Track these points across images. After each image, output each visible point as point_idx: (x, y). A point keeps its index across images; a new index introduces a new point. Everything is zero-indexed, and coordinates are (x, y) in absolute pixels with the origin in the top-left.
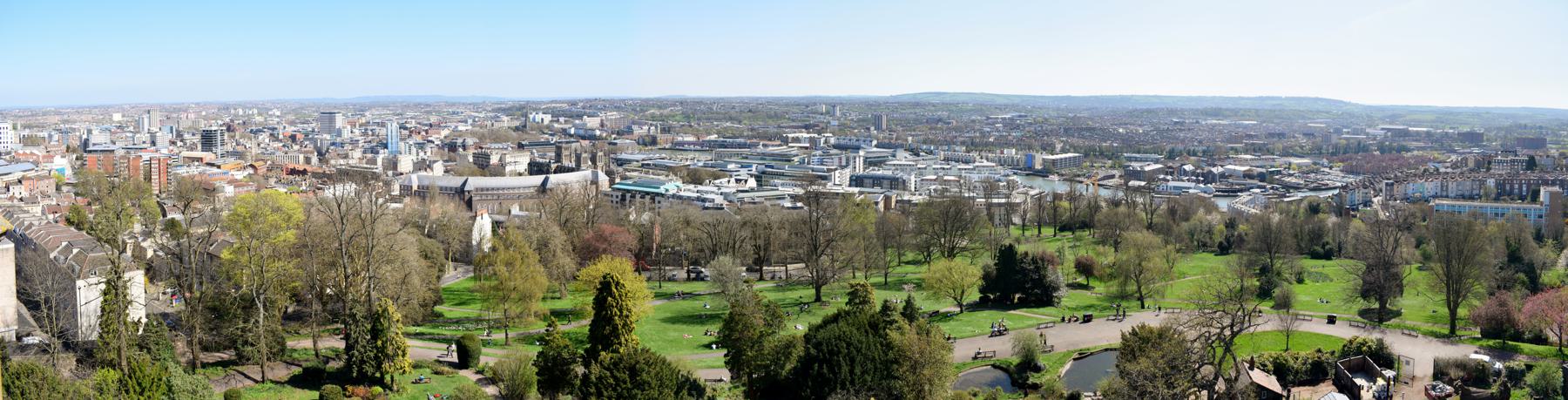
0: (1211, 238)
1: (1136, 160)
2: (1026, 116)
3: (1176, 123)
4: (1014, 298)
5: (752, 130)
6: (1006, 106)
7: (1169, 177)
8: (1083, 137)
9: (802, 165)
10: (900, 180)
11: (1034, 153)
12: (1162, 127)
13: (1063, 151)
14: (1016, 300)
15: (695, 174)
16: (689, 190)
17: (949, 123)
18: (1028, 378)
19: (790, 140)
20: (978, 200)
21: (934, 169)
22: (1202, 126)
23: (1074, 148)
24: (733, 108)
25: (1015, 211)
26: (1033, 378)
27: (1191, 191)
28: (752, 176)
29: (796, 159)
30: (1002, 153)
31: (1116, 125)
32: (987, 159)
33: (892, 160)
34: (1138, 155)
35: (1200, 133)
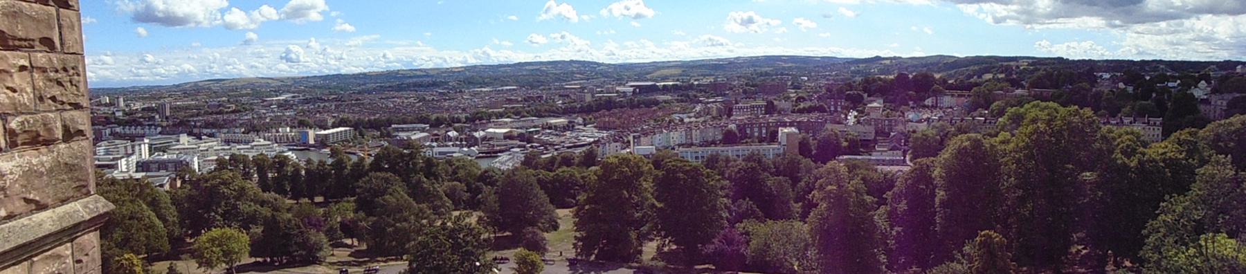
1: (403, 130)
7: (434, 144)
10: (184, 163)
13: (333, 127)
21: (216, 150)
27: (454, 155)
30: (278, 132)
33: (177, 145)
34: (404, 126)
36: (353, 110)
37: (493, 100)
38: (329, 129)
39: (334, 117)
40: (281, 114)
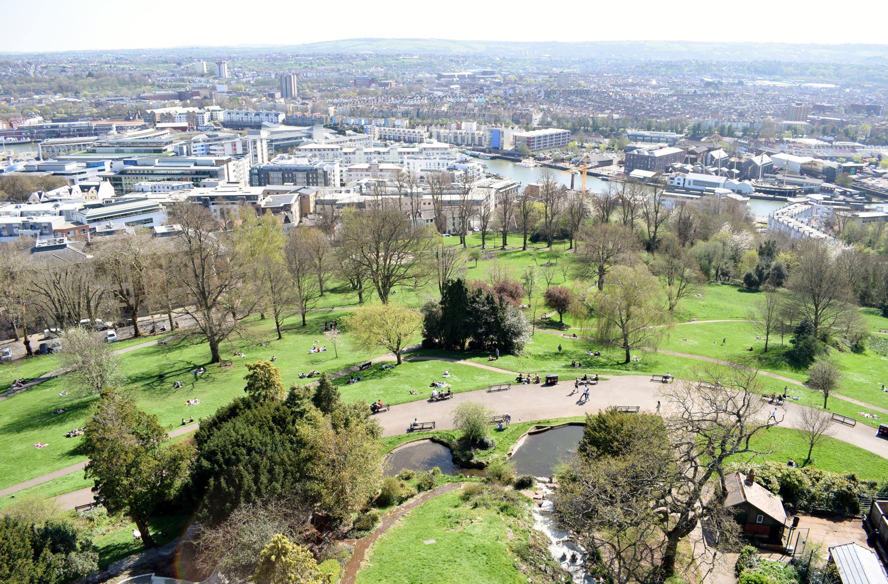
0: (736, 266)
1: (644, 139)
2: (492, 73)
3: (708, 84)
4: (464, 343)
5: (98, 104)
6: (466, 58)
7: (689, 167)
8: (572, 104)
9: (179, 158)
10: (320, 171)
11: (502, 129)
12: (686, 90)
13: (544, 124)
14: (467, 344)
15: (14, 185)
16: (8, 213)
17: (386, 85)
18: (472, 457)
19: (158, 119)
20: (425, 197)
21: (366, 153)
22: (748, 90)
23: (559, 121)
24: (63, 70)
25: (472, 213)
26: (478, 457)
27: (718, 190)
28: (105, 179)
29: (170, 148)
30: (459, 128)
31: (619, 86)
32: (439, 139)
33: (308, 143)
34: (646, 133)
35: (743, 101)
36: (571, 101)
37: (794, 105)
38: (534, 129)
39: (542, 110)
40: (466, 100)
